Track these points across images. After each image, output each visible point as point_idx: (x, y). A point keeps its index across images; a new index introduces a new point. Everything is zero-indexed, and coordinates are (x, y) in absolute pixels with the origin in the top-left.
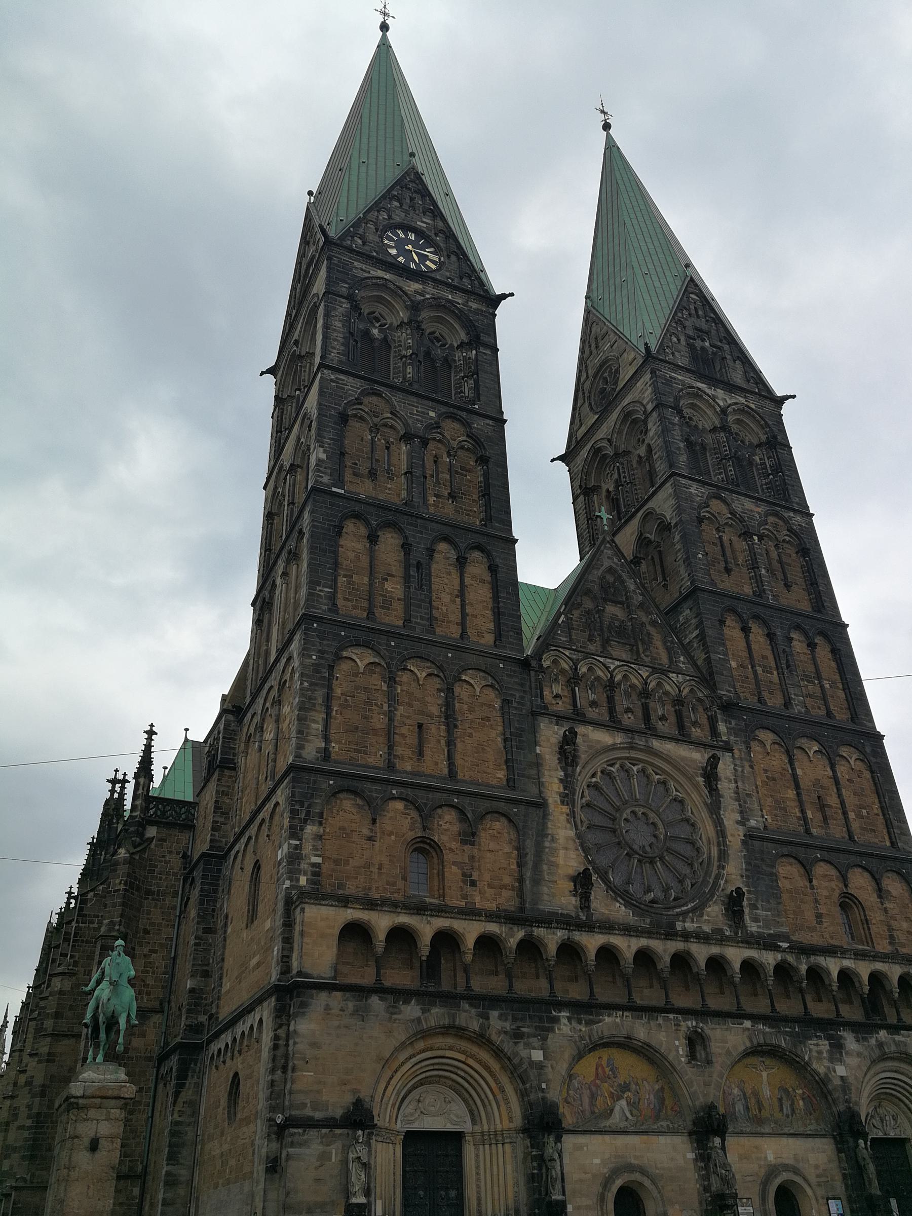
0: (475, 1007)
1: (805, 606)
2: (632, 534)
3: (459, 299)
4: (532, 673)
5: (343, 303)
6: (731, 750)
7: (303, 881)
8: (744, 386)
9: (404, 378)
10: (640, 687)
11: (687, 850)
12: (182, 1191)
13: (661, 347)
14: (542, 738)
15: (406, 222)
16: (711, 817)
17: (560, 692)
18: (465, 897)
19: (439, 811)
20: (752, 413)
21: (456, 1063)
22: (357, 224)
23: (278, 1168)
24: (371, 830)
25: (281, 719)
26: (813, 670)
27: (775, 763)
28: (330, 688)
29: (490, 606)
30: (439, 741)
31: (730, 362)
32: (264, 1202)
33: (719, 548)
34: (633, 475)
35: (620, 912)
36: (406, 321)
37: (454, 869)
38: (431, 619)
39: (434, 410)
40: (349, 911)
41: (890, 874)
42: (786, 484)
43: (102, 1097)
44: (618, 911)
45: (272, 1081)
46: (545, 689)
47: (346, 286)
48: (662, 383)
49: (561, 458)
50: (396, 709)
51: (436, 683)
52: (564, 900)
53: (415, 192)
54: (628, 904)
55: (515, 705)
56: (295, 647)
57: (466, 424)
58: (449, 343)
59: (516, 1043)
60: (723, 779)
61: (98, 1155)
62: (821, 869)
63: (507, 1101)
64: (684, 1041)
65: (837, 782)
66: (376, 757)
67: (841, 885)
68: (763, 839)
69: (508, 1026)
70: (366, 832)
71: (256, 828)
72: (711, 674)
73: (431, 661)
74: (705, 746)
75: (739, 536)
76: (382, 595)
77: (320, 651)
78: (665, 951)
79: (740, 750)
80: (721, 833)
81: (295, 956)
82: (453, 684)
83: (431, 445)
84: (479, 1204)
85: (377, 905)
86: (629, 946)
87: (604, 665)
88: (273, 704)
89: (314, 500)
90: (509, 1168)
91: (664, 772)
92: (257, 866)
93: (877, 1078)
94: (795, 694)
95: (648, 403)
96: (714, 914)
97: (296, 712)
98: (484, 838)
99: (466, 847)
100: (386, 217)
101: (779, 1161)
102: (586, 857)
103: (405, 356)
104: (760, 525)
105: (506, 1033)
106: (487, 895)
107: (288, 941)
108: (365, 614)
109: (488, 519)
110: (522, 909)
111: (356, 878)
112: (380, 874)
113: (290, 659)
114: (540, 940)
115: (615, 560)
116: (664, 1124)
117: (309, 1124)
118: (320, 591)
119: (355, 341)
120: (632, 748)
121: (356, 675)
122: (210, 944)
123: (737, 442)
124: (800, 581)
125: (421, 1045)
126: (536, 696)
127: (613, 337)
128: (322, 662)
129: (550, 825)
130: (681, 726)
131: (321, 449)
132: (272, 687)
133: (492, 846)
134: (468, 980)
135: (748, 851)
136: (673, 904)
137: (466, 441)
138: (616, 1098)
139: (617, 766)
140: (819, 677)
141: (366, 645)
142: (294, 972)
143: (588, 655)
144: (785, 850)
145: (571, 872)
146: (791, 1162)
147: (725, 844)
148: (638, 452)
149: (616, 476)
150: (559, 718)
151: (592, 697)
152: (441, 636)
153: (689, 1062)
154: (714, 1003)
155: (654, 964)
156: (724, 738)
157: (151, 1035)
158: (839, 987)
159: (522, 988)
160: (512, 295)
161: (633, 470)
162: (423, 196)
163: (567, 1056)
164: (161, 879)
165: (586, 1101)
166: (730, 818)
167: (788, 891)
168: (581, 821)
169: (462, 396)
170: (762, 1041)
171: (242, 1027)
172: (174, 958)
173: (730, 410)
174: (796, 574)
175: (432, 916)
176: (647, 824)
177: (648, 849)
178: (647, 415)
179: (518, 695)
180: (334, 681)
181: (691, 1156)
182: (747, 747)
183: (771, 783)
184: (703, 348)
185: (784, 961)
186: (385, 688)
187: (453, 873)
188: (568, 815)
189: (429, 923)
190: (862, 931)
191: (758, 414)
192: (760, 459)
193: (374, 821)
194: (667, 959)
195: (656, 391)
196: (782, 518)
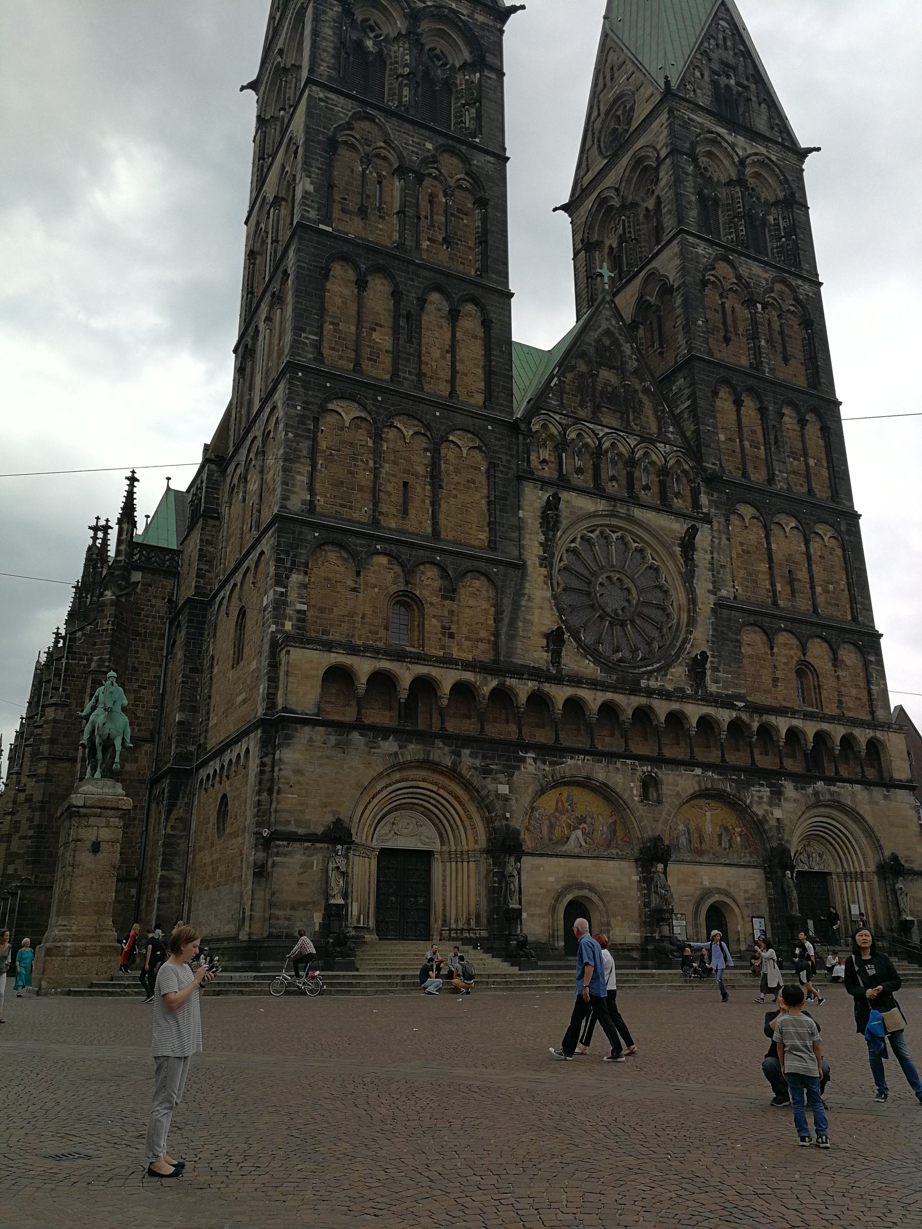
0: (449, 746)
1: (801, 381)
2: (632, 296)
4: (521, 437)
5: (334, 5)
6: (710, 522)
7: (288, 626)
8: (767, 134)
9: (400, 102)
10: (627, 456)
11: (657, 615)
12: (175, 892)
13: (683, 83)
14: (526, 502)
16: (684, 586)
17: (547, 457)
18: (443, 647)
19: (422, 567)
21: (428, 793)
23: (265, 874)
24: (356, 582)
25: (265, 471)
26: (800, 446)
27: (751, 537)
28: (315, 440)
29: (482, 364)
30: (424, 501)
31: (755, 105)
32: (253, 899)
33: (720, 316)
34: (639, 230)
35: (589, 668)
36: (403, 32)
37: (434, 621)
38: (420, 375)
39: (430, 140)
40: (333, 655)
41: (846, 646)
42: (798, 248)
43: (100, 808)
45: (259, 801)
46: (532, 453)
48: (680, 125)
49: (564, 208)
50: (381, 467)
51: (422, 442)
52: (536, 655)
54: (597, 662)
55: (501, 468)
56: (279, 396)
57: (465, 160)
58: (451, 62)
59: (484, 778)
60: (699, 550)
61: (99, 856)
62: (783, 638)
63: (473, 827)
65: (809, 559)
66: (361, 513)
67: (800, 654)
68: (730, 608)
69: (477, 762)
70: (350, 583)
71: (241, 576)
72: (699, 446)
73: (418, 420)
74: (685, 516)
75: (742, 304)
76: (370, 347)
77: (305, 402)
78: (628, 705)
79: (719, 523)
80: (693, 601)
81: (280, 693)
82: (440, 444)
83: (425, 183)
84: (444, 910)
85: (360, 651)
86: (595, 699)
88: (256, 455)
89: (300, 236)
90: (472, 881)
91: (642, 539)
92: (242, 612)
93: (810, 821)
95: (662, 148)
96: (677, 675)
97: (281, 463)
98: (464, 594)
99: (446, 602)
101: (713, 885)
103: (402, 76)
104: (765, 292)
105: (476, 769)
106: (464, 647)
107: (273, 680)
108: (351, 366)
109: (484, 270)
110: (496, 661)
111: (340, 626)
112: (363, 623)
113: (274, 408)
114: (511, 688)
115: (614, 322)
116: (614, 851)
117: (292, 838)
119: (346, 53)
120: (613, 515)
121: (342, 429)
122: (197, 683)
123: (752, 198)
125: (397, 776)
126: (523, 461)
127: (630, 67)
128: (307, 413)
129: (527, 585)
130: (663, 496)
131: (308, 180)
132: (255, 437)
133: (471, 603)
134: (443, 723)
135: (716, 618)
136: (639, 663)
137: (465, 179)
138: (572, 828)
139: (597, 532)
140: (805, 455)
141: (352, 398)
142: (280, 708)
143: (577, 421)
144: (752, 619)
145: (546, 630)
146: (724, 886)
147: (694, 609)
148: (645, 205)
149: (620, 231)
150: (545, 483)
151: (579, 463)
152: (430, 394)
153: (642, 801)
154: (668, 753)
155: (617, 717)
156: (705, 510)
157: (143, 761)
158: (786, 743)
159: (493, 730)
160: (523, 7)
161: (638, 225)
163: (530, 791)
164: (147, 621)
166: (702, 586)
167: (750, 657)
168: (558, 583)
170: (709, 786)
171: (228, 756)
172: (163, 695)
173: (749, 161)
174: (796, 348)
175: (410, 662)
176: (621, 589)
177: (620, 612)
178: (660, 162)
179: (504, 458)
180: (319, 434)
181: (636, 878)
182: (726, 520)
183: (746, 556)
184: (727, 87)
185: (738, 718)
186: (371, 444)
187: (433, 625)
189: (408, 669)
190: (813, 696)
191: (778, 168)
192: (775, 219)
193: (358, 574)
194: (630, 712)
195: (672, 134)
196: (789, 286)
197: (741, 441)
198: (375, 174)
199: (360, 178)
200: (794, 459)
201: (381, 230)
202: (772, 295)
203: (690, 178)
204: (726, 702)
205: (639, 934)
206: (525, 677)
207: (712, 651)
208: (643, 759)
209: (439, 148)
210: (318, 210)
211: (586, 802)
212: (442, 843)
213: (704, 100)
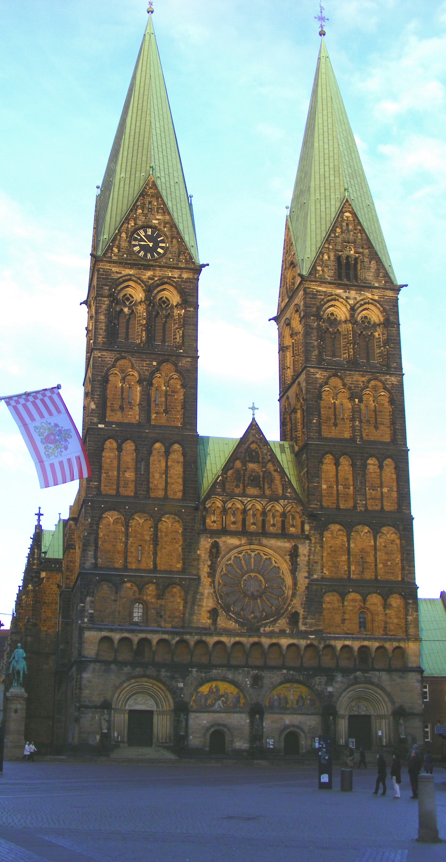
1: (387, 438)
3: (176, 274)
13: (313, 269)
14: (201, 546)
15: (145, 224)
17: (215, 519)
19: (147, 586)
20: (375, 303)
22: (114, 240)
26: (379, 482)
29: (182, 475)
30: (149, 553)
33: (333, 409)
35: (232, 625)
37: (153, 611)
38: (148, 490)
39: (155, 360)
40: (103, 633)
44: (231, 625)
47: (107, 288)
48: (310, 298)
53: (153, 196)
54: (236, 621)
55: (189, 530)
58: (171, 303)
60: (301, 555)
63: (169, 701)
64: (250, 679)
67: (362, 604)
69: (168, 674)
70: (113, 598)
77: (92, 517)
78: (248, 642)
79: (316, 538)
80: (295, 584)
82: (157, 524)
86: (230, 641)
87: (241, 501)
90: (168, 723)
94: (361, 501)
96: (282, 623)
99: (159, 601)
100: (133, 225)
102: (218, 602)
108: (115, 492)
115: (257, 436)
116: (238, 709)
117: (87, 707)
118: (92, 485)
120: (250, 544)
123: (365, 323)
124: (387, 421)
125: (133, 681)
126: (200, 525)
129: (201, 588)
130: (283, 528)
138: (216, 700)
139: (243, 554)
140: (381, 487)
141: (114, 510)
145: (209, 609)
151: (233, 519)
156: (306, 533)
160: (208, 265)
162: (157, 199)
165: (203, 701)
166: (302, 575)
167: (329, 609)
169: (176, 342)
173: (358, 305)
174: (386, 419)
175: (138, 633)
181: (248, 721)
182: (320, 536)
183: (333, 554)
186: (123, 530)
187: (152, 612)
188: (210, 582)
189: (136, 636)
191: (379, 304)
192: (379, 335)
193: (117, 593)
195: (306, 305)
196: (380, 381)
197: (337, 487)
198: (128, 386)
199: (120, 390)
200: (373, 490)
201: (131, 415)
202: (368, 389)
203: (314, 331)
204: (304, 635)
205: (248, 745)
206: (194, 634)
207: (304, 608)
208: (254, 667)
209: (159, 364)
210: (98, 417)
211: (224, 687)
212: (158, 706)
213: (329, 275)
